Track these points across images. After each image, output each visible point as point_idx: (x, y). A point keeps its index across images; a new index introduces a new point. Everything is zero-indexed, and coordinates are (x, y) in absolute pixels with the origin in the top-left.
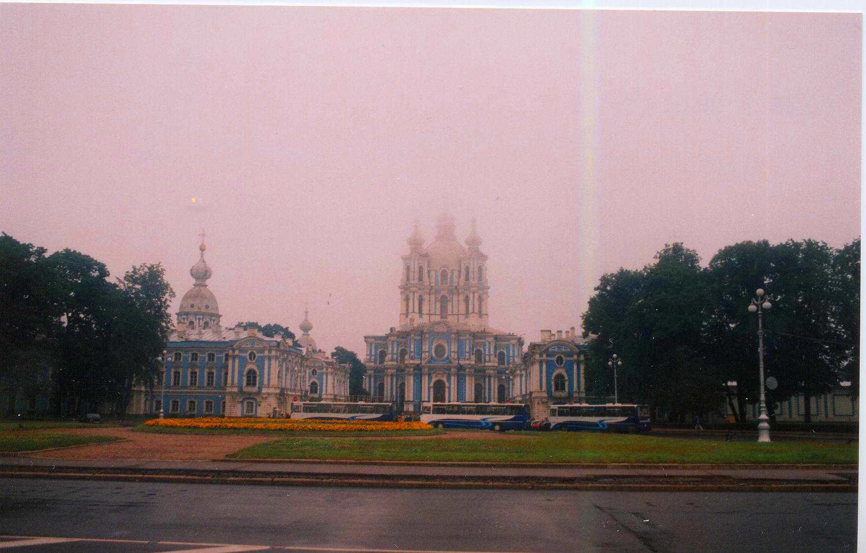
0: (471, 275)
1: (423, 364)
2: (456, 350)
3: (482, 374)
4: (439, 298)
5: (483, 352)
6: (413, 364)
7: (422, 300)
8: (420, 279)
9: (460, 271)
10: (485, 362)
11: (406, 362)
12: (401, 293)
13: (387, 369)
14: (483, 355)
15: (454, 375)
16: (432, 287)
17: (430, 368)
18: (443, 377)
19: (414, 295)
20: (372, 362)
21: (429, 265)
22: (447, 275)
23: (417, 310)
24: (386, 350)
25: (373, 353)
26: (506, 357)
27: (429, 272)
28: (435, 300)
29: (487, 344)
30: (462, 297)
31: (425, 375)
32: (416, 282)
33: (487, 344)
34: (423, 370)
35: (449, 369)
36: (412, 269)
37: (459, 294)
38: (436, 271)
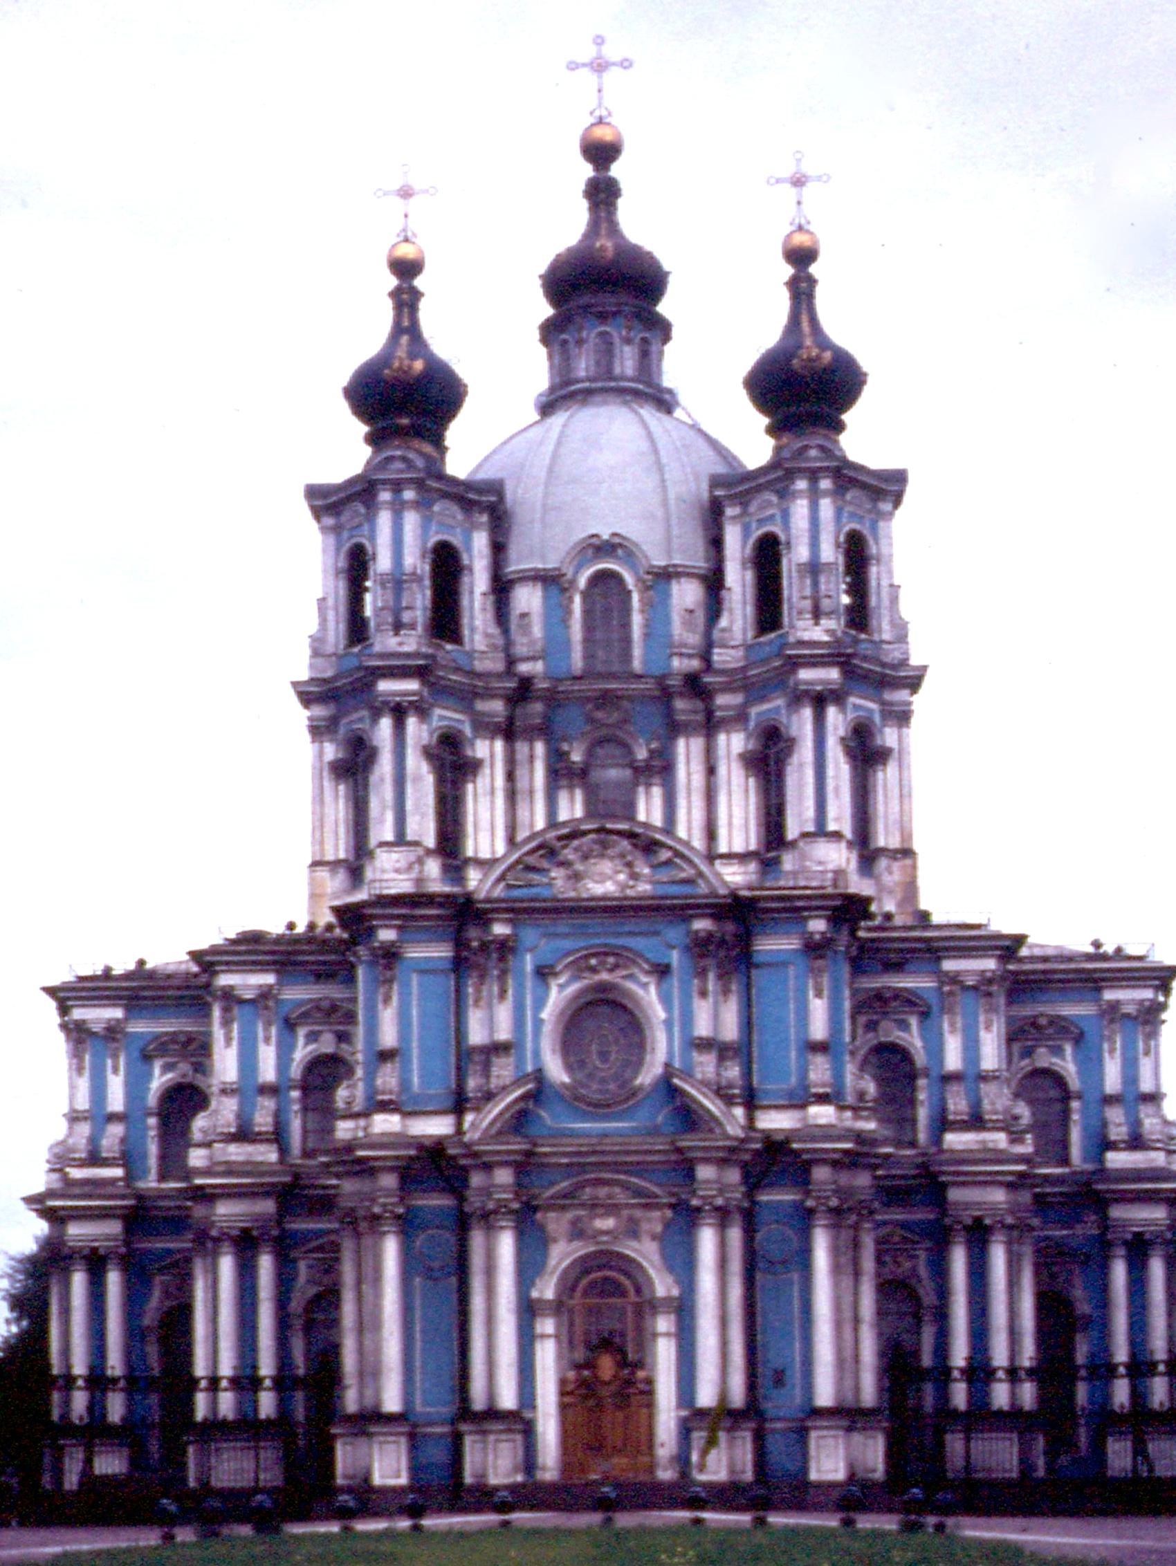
0: (793, 589)
3: (922, 1215)
9: (714, 583)
10: (942, 1123)
11: (344, 1129)
12: (318, 731)
13: (206, 1196)
15: (723, 1216)
17: (525, 1165)
19: (399, 726)
24: (200, 1081)
27: (501, 588)
30: (733, 743)
31: (488, 1219)
32: (411, 643)
34: (476, 1180)
35: (685, 1167)
36: (383, 562)
37: (710, 726)
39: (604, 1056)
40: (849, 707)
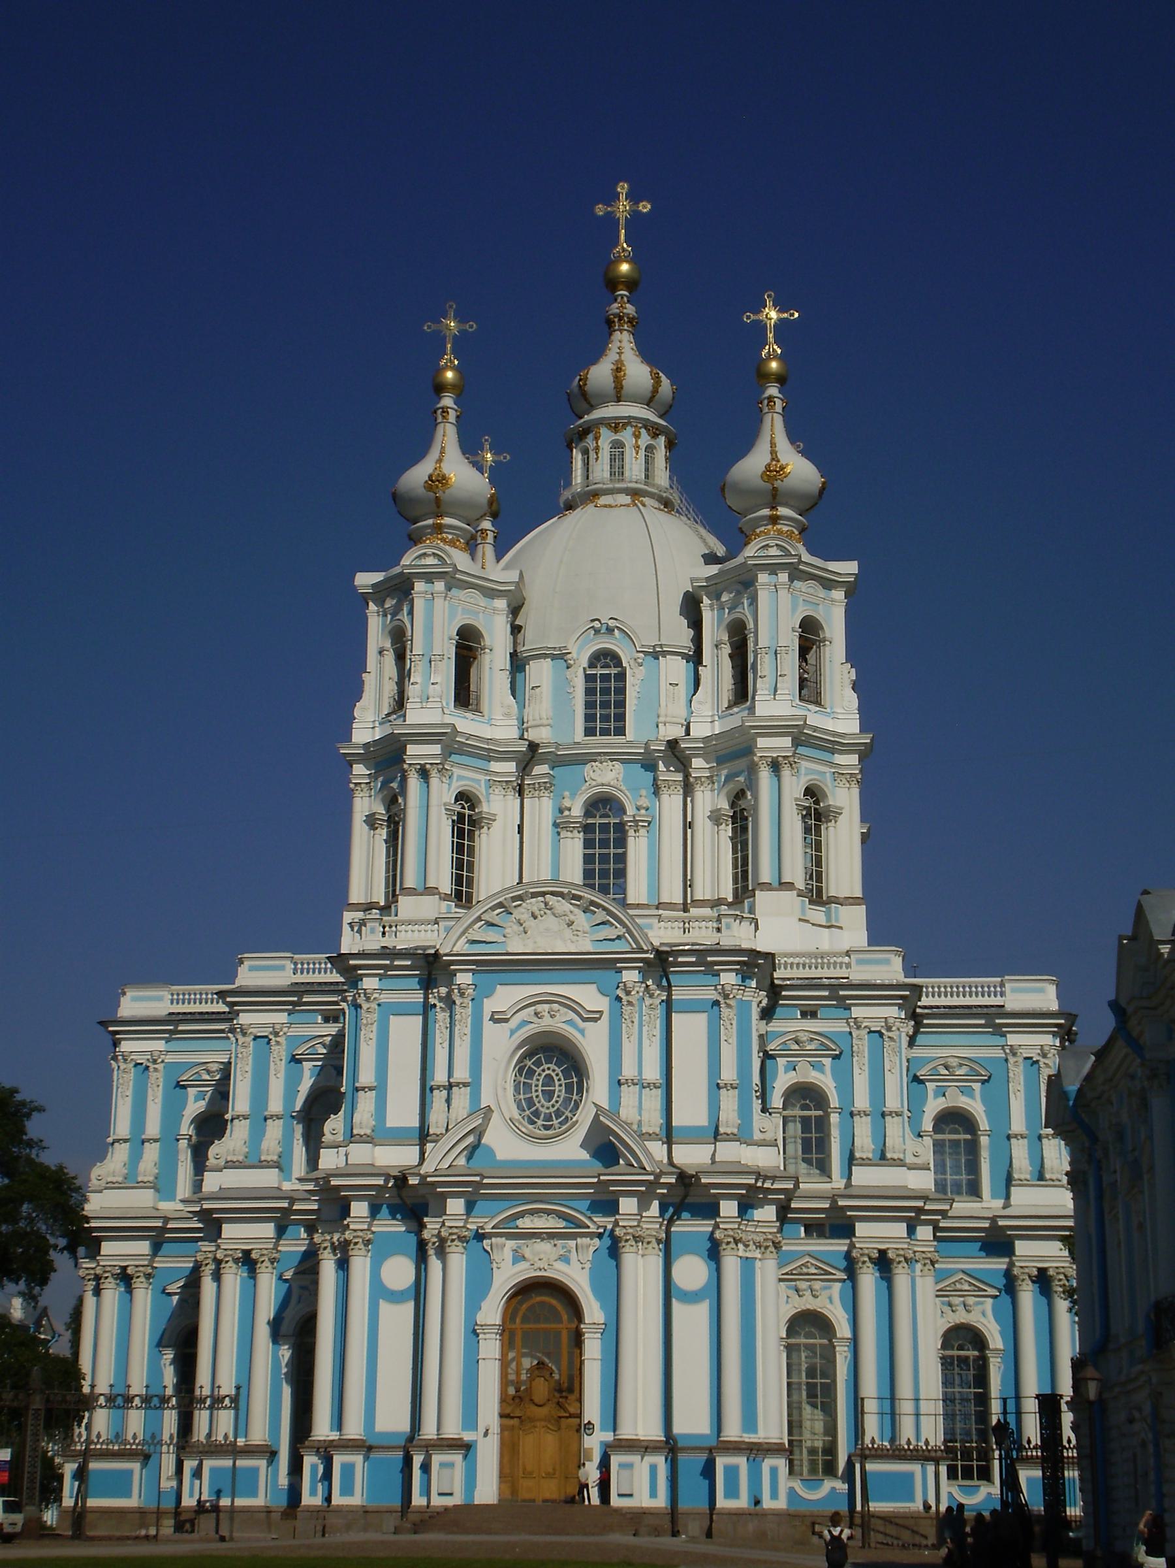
1: (428, 1168)
2: (652, 1072)
4: (577, 811)
5: (834, 1102)
6: (371, 1171)
7: (473, 823)
8: (464, 696)
14: (834, 1118)
16: (533, 747)
18: (565, 1259)
20: (141, 1185)
21: (516, 630)
22: (621, 677)
23: (443, 877)
25: (153, 1128)
26: (984, 1140)
28: (556, 825)
29: (862, 1043)
33: (862, 1043)
38: (560, 656)
39: (549, 1095)
40: (803, 771)
